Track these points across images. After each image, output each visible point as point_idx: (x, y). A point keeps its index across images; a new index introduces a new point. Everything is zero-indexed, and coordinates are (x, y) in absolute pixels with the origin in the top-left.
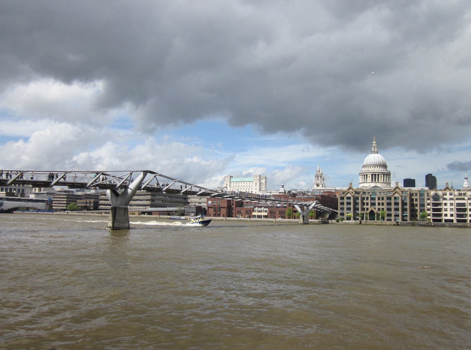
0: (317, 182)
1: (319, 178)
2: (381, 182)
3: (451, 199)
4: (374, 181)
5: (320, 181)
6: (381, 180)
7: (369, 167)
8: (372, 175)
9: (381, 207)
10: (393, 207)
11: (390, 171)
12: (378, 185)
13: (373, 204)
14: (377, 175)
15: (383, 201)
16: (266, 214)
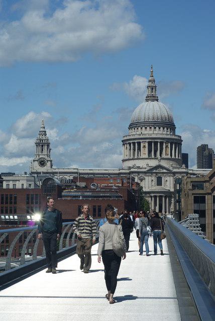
0: (40, 156)
1: (45, 148)
2: (167, 157)
4: (153, 157)
5: (47, 155)
6: (166, 154)
7: (144, 128)
8: (150, 144)
11: (181, 137)
12: (164, 163)
14: (159, 144)
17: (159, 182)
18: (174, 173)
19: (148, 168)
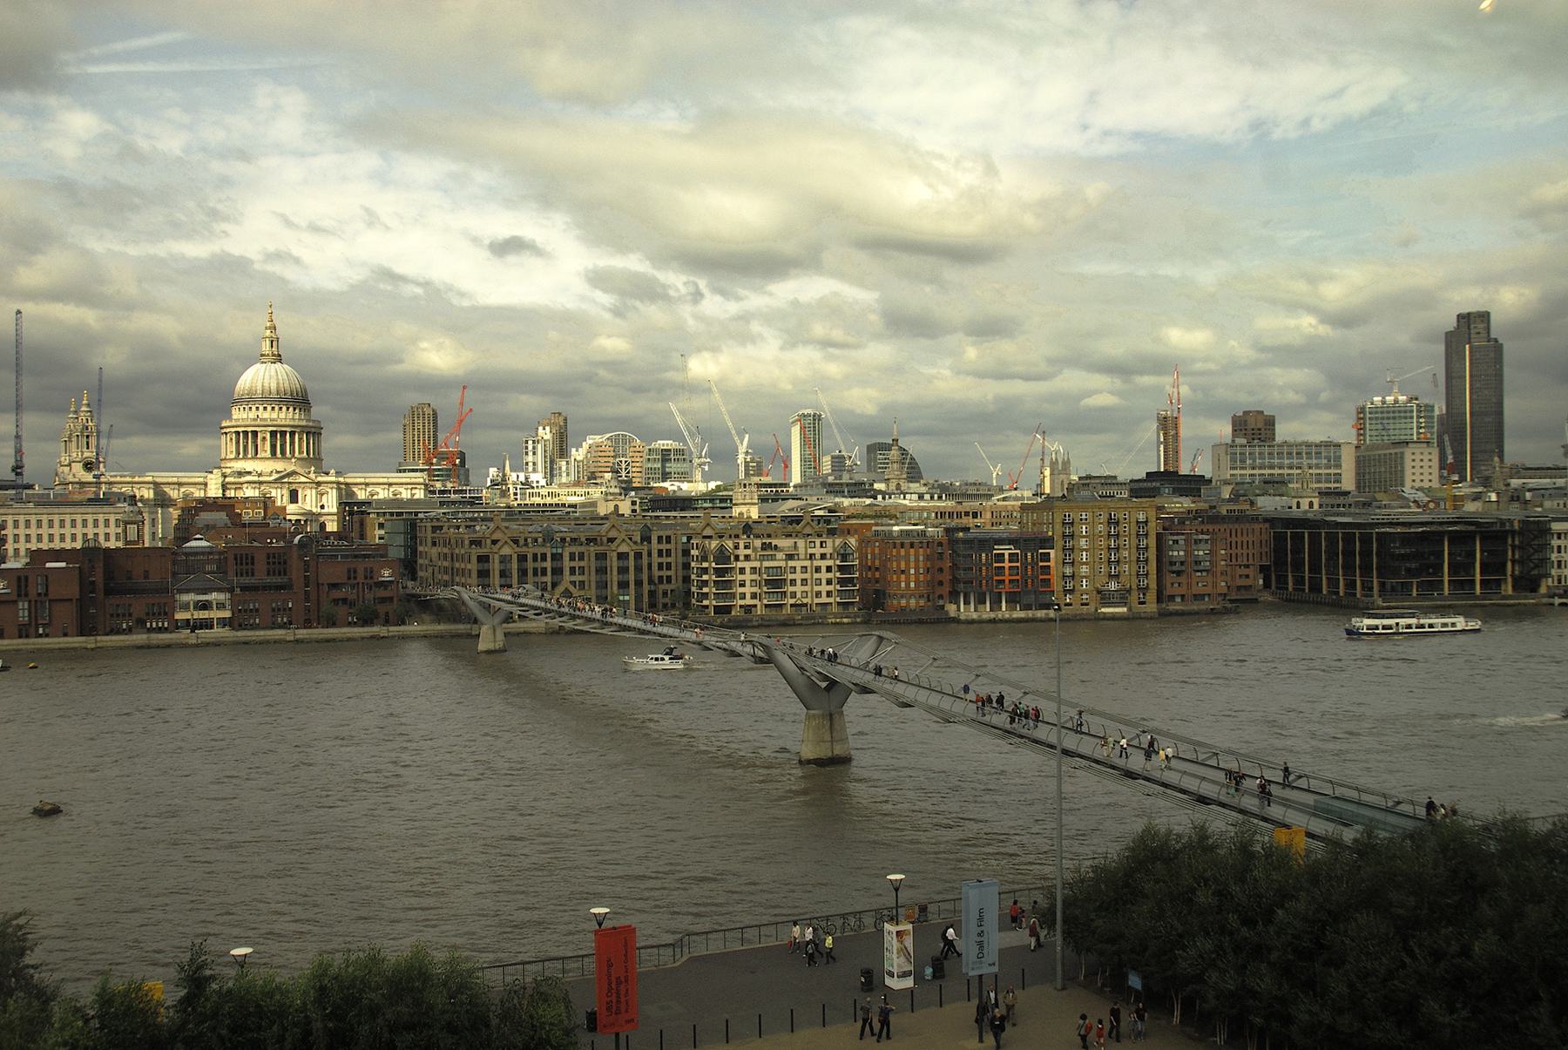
3: (747, 558)
8: (273, 434)
9: (577, 578)
10: (614, 577)
13: (557, 571)
15: (582, 564)
16: (227, 614)
17: (294, 497)
18: (319, 484)
19: (275, 476)
